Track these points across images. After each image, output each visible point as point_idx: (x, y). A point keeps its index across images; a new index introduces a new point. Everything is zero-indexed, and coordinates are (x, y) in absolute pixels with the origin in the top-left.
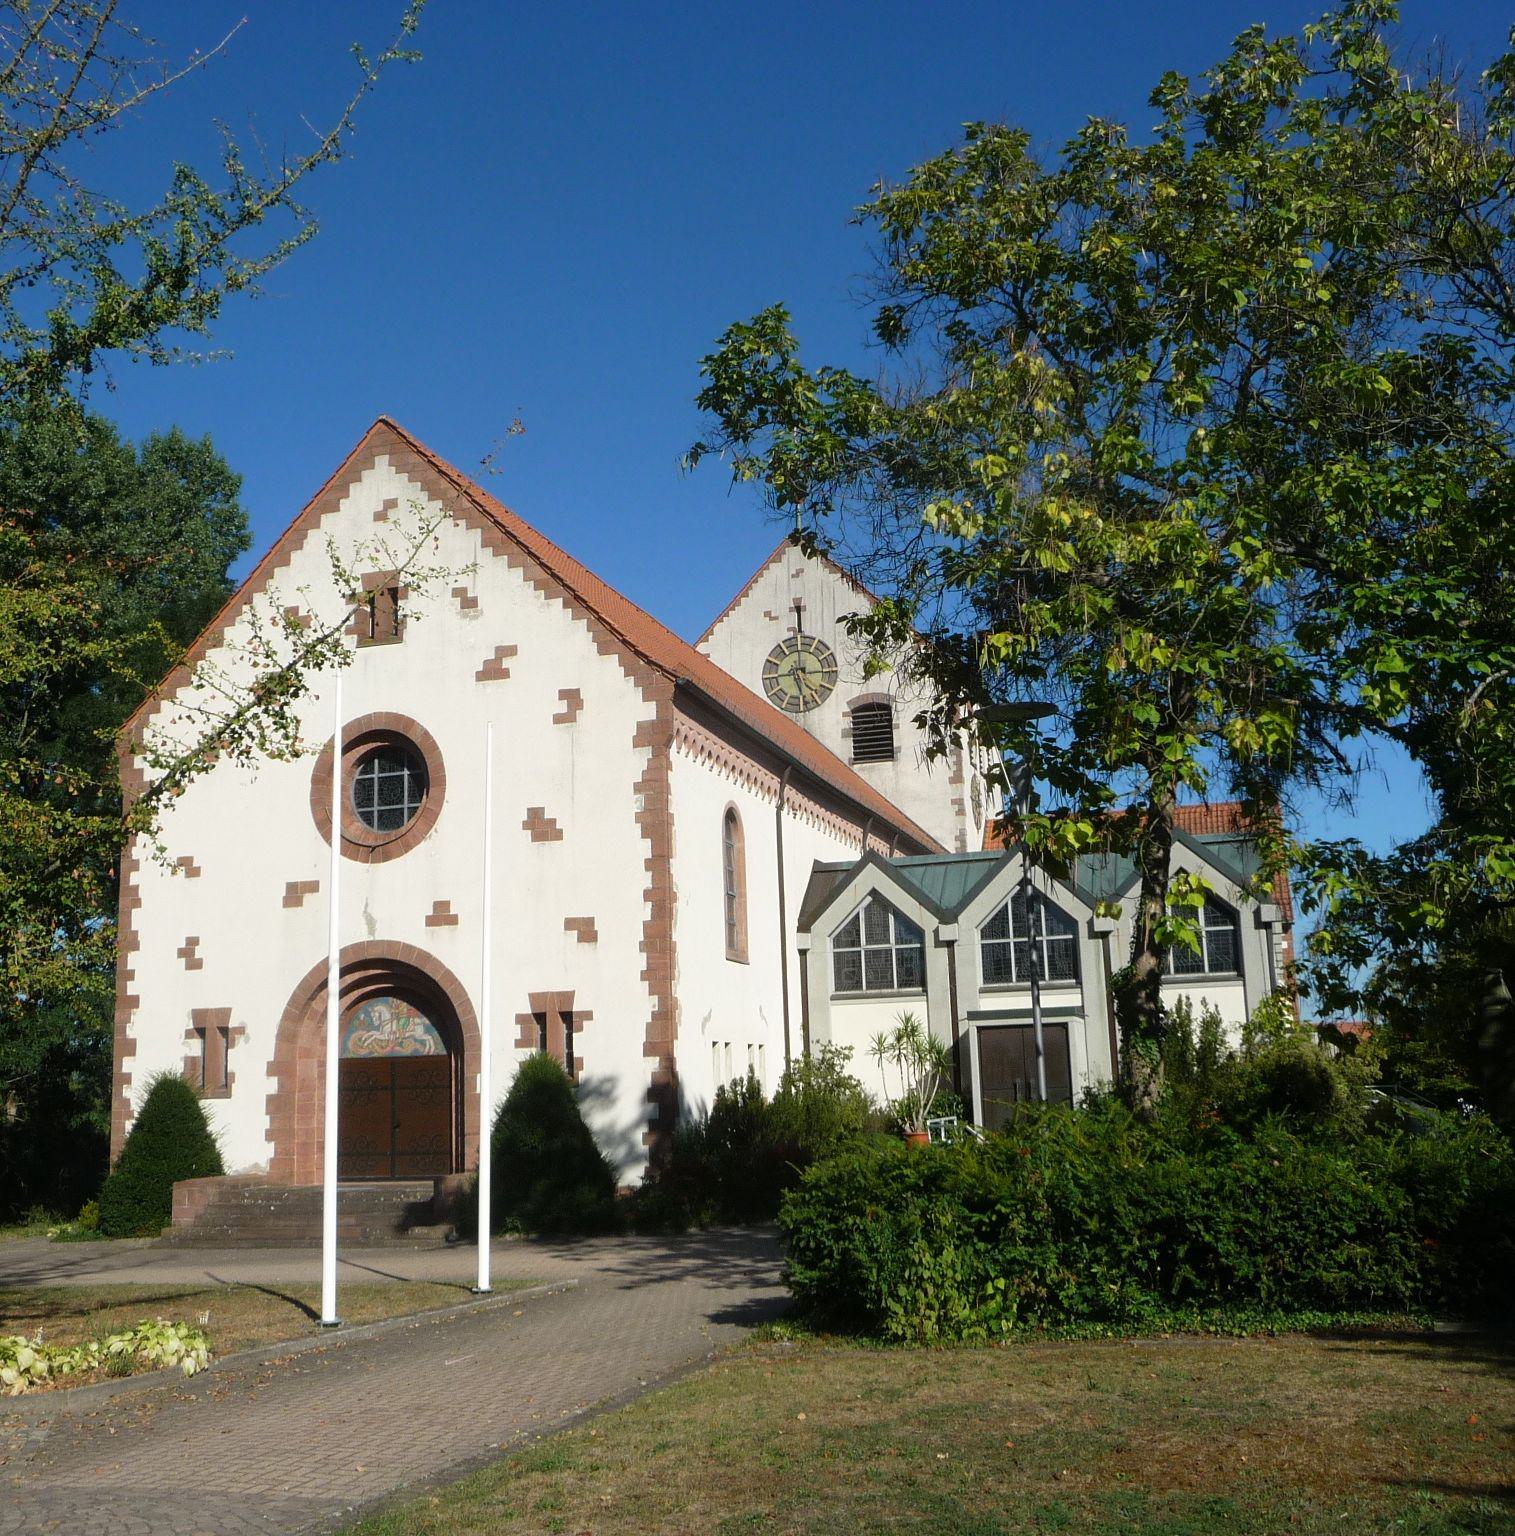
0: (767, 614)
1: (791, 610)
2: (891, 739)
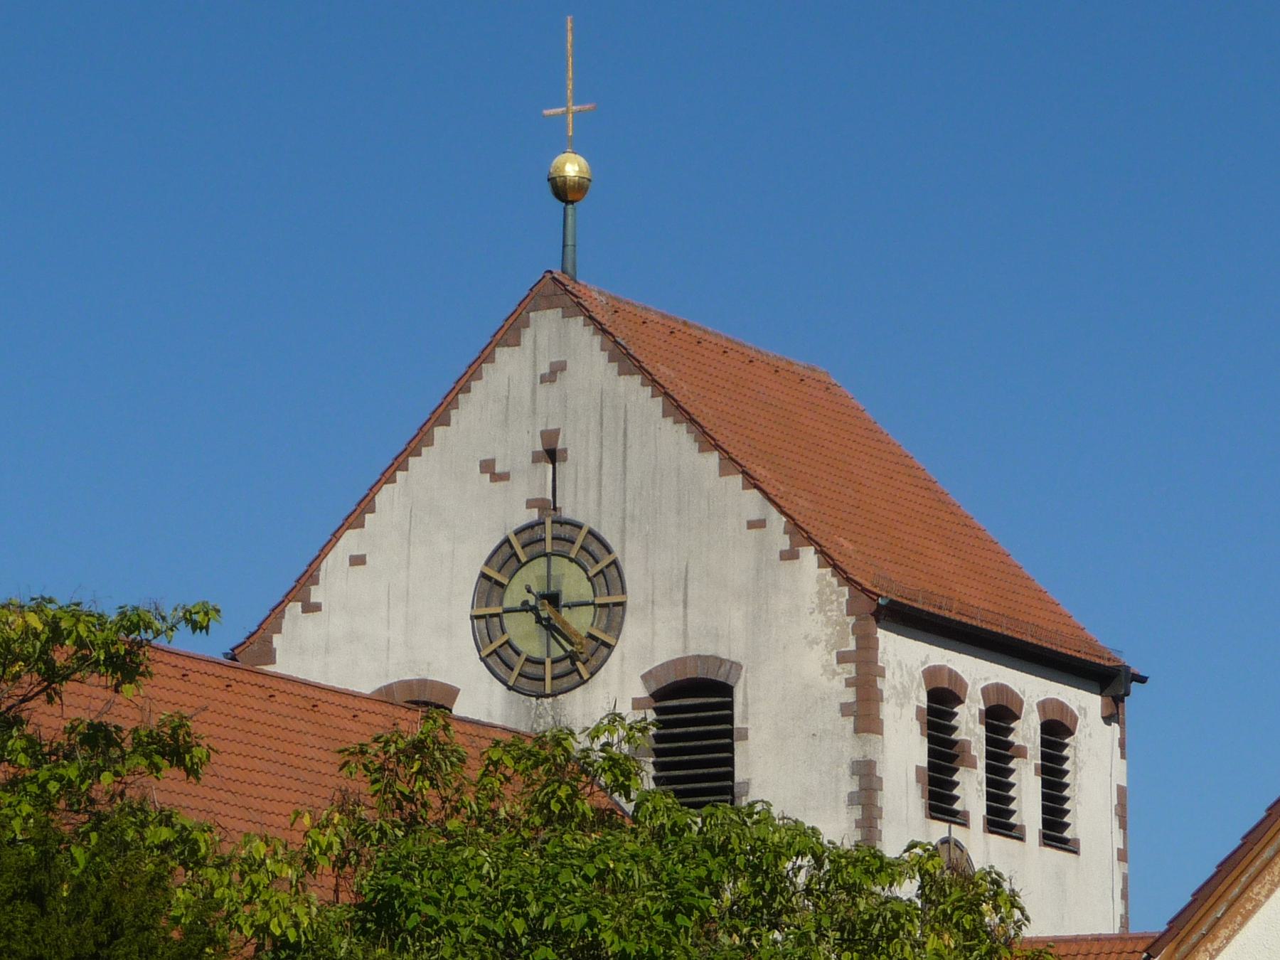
0: (487, 466)
1: (536, 458)
2: (730, 762)
